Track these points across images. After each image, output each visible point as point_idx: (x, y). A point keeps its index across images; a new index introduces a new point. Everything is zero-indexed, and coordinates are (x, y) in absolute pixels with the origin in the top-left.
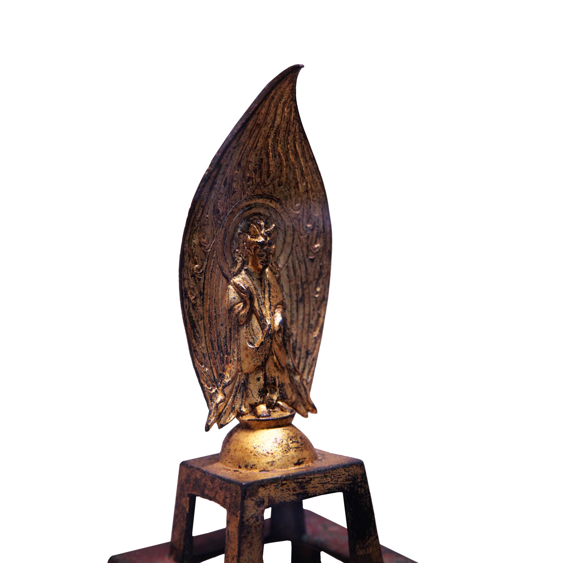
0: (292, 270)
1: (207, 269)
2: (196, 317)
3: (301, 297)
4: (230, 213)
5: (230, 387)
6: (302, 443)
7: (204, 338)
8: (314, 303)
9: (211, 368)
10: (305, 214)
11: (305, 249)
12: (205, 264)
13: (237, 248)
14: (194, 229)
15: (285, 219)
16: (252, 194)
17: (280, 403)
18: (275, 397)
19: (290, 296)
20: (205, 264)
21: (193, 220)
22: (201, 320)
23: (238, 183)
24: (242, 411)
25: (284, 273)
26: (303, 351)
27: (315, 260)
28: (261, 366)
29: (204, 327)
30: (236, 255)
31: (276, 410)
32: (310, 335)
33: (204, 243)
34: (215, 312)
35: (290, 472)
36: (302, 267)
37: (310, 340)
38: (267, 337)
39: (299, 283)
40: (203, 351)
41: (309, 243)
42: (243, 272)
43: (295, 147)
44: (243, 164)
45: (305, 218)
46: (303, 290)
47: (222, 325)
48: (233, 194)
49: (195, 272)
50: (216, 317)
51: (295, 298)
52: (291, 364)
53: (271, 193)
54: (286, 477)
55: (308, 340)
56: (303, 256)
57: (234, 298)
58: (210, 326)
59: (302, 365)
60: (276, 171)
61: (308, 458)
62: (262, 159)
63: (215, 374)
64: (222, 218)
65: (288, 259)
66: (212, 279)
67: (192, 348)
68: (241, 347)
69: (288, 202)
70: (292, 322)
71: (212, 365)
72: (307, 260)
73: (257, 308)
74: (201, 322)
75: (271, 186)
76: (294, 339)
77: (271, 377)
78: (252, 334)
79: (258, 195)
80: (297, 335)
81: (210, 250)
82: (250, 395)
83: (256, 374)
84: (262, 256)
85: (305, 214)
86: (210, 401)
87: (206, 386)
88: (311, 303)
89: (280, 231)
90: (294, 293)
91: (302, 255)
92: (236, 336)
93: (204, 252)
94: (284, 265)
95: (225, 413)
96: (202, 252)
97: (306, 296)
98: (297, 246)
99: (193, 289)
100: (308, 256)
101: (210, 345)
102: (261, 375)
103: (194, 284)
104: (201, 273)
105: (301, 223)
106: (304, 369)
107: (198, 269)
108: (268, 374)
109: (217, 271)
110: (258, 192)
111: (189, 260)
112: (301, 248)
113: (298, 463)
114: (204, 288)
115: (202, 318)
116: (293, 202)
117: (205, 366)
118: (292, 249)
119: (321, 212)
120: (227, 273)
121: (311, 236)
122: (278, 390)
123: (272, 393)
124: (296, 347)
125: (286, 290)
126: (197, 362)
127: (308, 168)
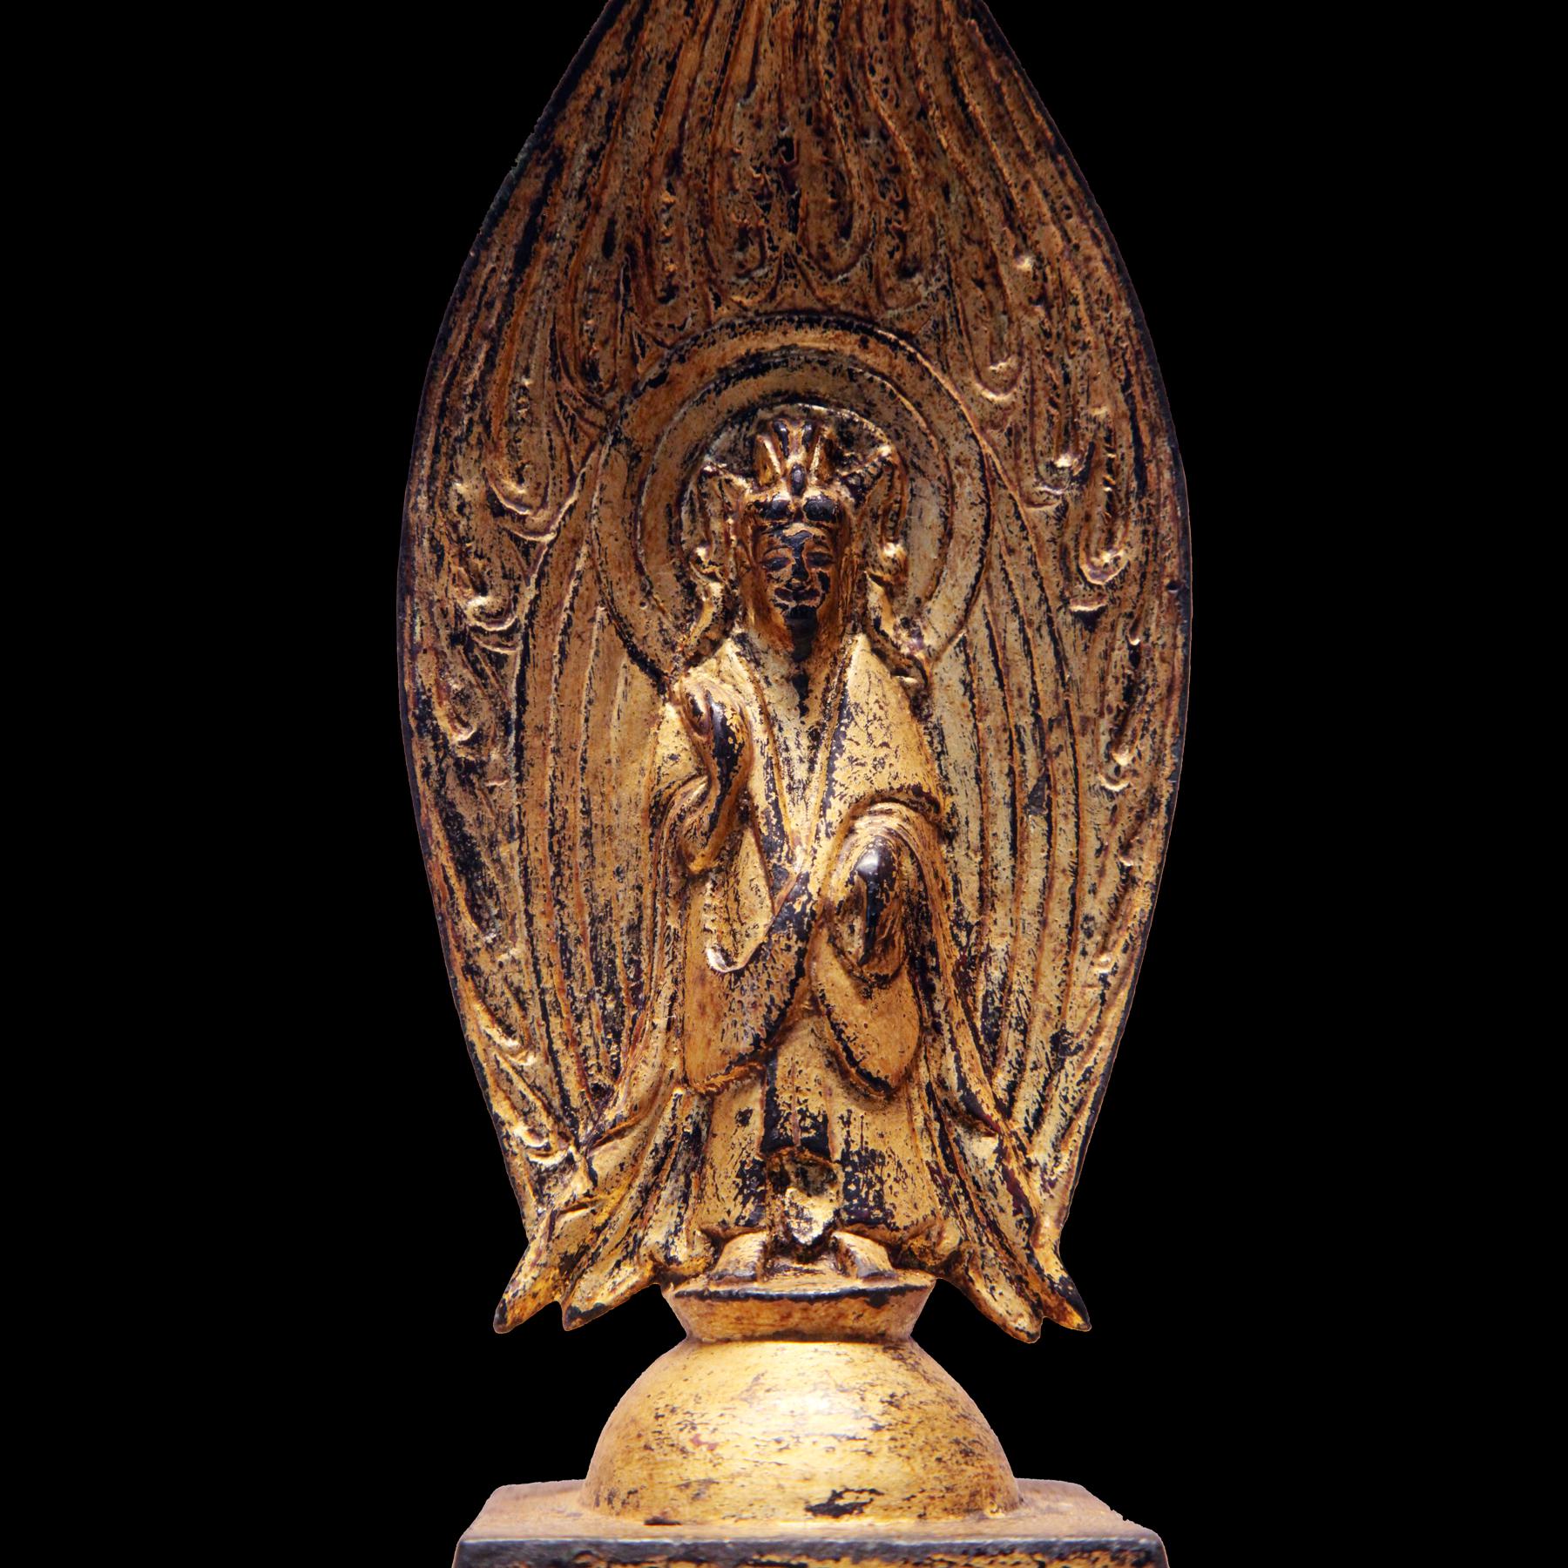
0: (985, 662)
1: (539, 619)
2: (480, 822)
3: (1036, 788)
4: (654, 383)
5: (624, 1146)
6: (883, 1421)
7: (521, 919)
8: (1102, 817)
9: (552, 1056)
10: (1043, 406)
11: (1048, 567)
12: (529, 593)
13: (704, 542)
14: (457, 433)
15: (940, 425)
16: (769, 307)
17: (847, 1238)
18: (820, 1211)
19: (978, 779)
20: (529, 593)
21: (446, 393)
22: (510, 837)
23: (682, 248)
24: (671, 1260)
25: (949, 672)
26: (1040, 1035)
27: (1105, 621)
28: (753, 1056)
29: (525, 872)
30: (701, 581)
31: (820, 1266)
32: (1078, 962)
33: (518, 501)
34: (587, 813)
35: (724, 1532)
36: (1036, 652)
37: (1076, 990)
38: (783, 925)
39: (1026, 721)
40: (516, 978)
41: (1068, 539)
42: (730, 648)
43: (956, 91)
44: (692, 159)
45: (1042, 422)
46: (1046, 755)
47: (618, 872)
48: (664, 300)
49: (474, 622)
50: (587, 834)
51: (1001, 789)
52: (953, 1080)
53: (866, 307)
54: (696, 1546)
55: (1066, 986)
56: (1044, 600)
57: (673, 757)
58: (558, 873)
59: (1027, 1097)
60: (873, 201)
61: (897, 1494)
62: (787, 147)
63: (572, 1084)
64: (611, 400)
65: (968, 611)
66: (570, 666)
67: (458, 960)
68: (691, 974)
69: (951, 348)
70: (986, 900)
71: (558, 1045)
72: (1062, 619)
73: (761, 801)
74: (506, 850)
75: (857, 272)
76: (996, 975)
77: (804, 1114)
78: (733, 919)
79: (795, 311)
80: (1011, 958)
81: (549, 538)
82: (710, 1190)
83: (736, 1093)
84: (778, 567)
85: (1043, 406)
86: (533, 1200)
87: (519, 1130)
88: (1087, 818)
89: (920, 482)
90: (997, 768)
91: (1035, 595)
92: (673, 922)
93: (517, 540)
94: (950, 640)
95: (594, 1259)
96: (506, 539)
97: (1064, 783)
98: (1011, 551)
99: (462, 698)
100: (1066, 602)
101: (556, 957)
102: (754, 1100)
103: (469, 676)
104: (508, 635)
105: (1024, 448)
106: (1039, 1117)
107: (483, 613)
108: (784, 1097)
109: (598, 631)
110: (795, 295)
111: (438, 567)
112: (1033, 562)
113: (832, 1508)
114: (522, 701)
115: (517, 832)
116: (981, 351)
117: (528, 1044)
118: (984, 564)
119: (1120, 396)
120: (654, 648)
121: (1074, 512)
122: (841, 1178)
123: (812, 1189)
124: (1000, 1013)
125: (959, 749)
126: (484, 1020)
127: (1035, 188)
